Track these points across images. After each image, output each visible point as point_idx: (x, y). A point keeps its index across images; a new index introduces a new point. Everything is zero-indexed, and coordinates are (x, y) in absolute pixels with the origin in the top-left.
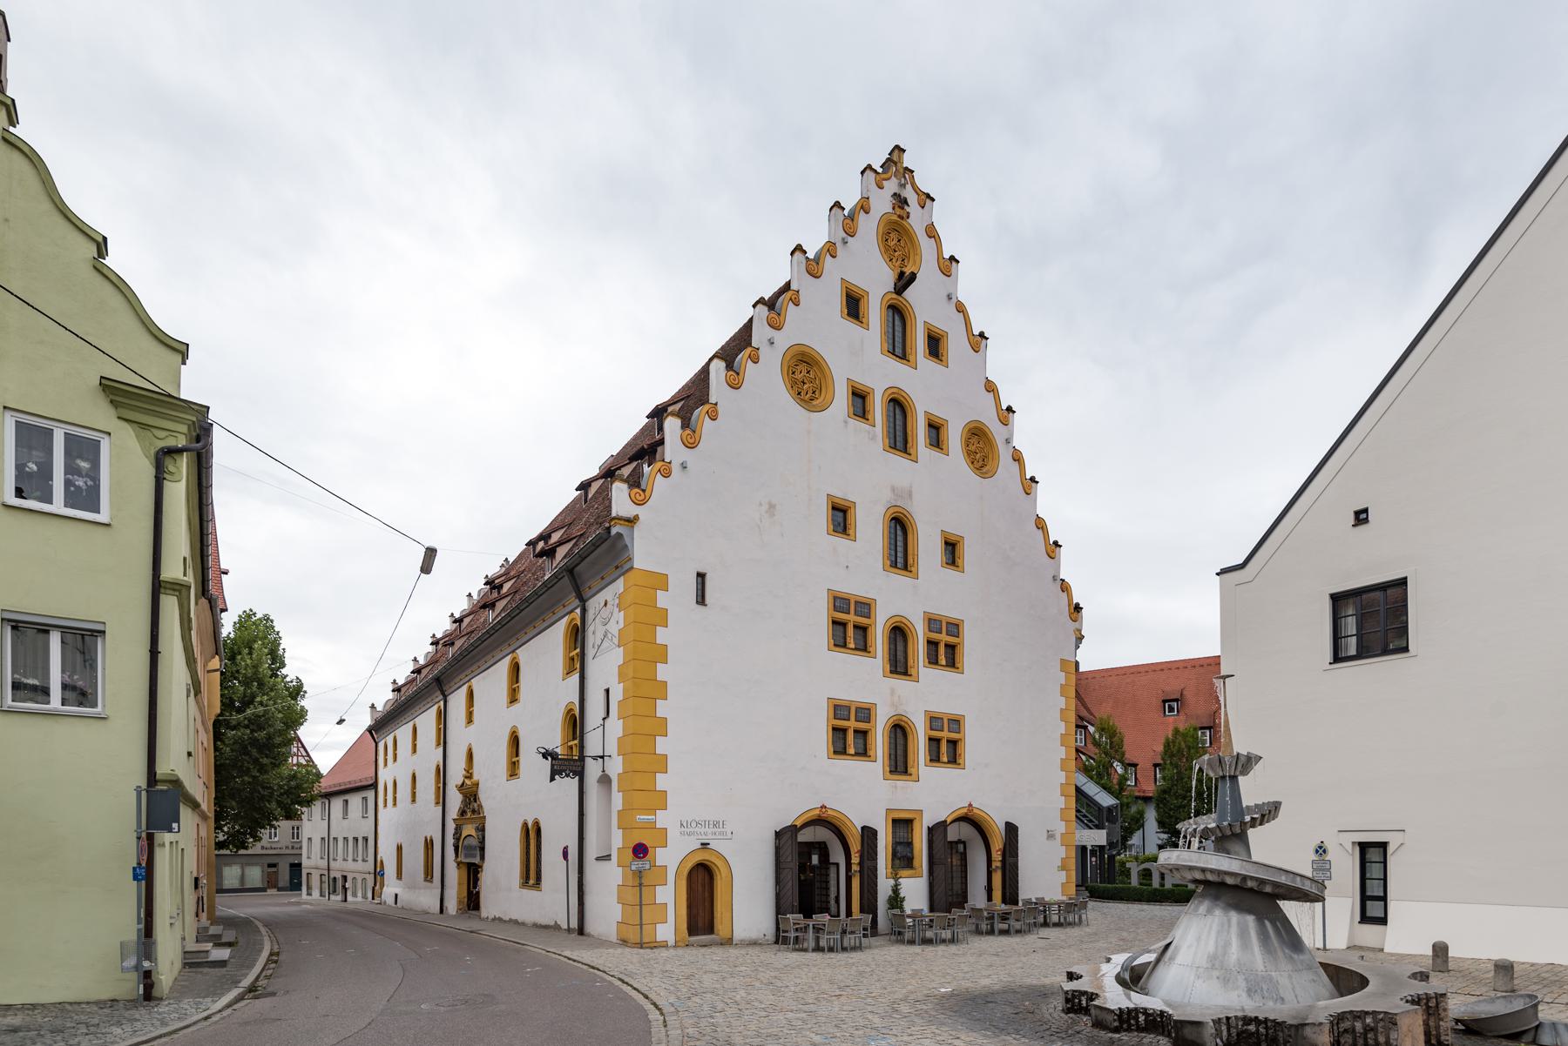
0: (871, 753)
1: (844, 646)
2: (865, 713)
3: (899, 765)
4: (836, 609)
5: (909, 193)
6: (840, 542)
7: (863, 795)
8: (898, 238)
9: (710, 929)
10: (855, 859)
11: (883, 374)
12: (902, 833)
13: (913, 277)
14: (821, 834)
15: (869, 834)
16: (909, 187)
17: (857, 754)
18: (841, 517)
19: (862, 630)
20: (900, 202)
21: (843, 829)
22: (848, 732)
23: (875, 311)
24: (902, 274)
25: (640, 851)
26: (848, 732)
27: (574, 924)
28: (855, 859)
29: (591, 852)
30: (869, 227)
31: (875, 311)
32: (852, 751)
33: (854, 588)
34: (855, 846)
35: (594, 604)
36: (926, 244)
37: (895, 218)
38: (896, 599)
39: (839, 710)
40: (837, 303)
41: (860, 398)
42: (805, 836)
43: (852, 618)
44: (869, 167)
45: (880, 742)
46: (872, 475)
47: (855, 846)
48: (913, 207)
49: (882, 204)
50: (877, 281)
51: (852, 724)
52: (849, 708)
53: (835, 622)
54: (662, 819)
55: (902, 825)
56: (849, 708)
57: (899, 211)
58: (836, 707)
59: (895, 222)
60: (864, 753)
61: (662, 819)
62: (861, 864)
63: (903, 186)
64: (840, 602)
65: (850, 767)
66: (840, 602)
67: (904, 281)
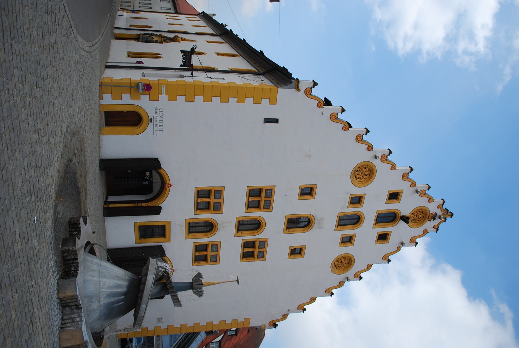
0: (198, 211)
2: (218, 208)
5: (438, 221)
7: (177, 208)
8: (421, 216)
10: (144, 204)
11: (369, 210)
13: (407, 222)
15: (157, 211)
16: (440, 220)
17: (198, 203)
20: (434, 217)
22: (208, 198)
24: (408, 218)
25: (148, 87)
26: (208, 198)
28: (144, 204)
29: (146, 72)
33: (277, 199)
34: (150, 204)
35: (262, 77)
37: (428, 215)
38: (273, 221)
39: (219, 193)
40: (395, 188)
41: (357, 200)
42: (156, 179)
43: (263, 199)
45: (204, 216)
46: (326, 208)
47: (150, 204)
49: (433, 208)
51: (212, 200)
52: (220, 199)
54: (163, 98)
56: (220, 198)
57: (431, 216)
58: (221, 191)
60: (199, 207)
61: (163, 98)
62: (142, 206)
63: (440, 217)
67: (406, 219)
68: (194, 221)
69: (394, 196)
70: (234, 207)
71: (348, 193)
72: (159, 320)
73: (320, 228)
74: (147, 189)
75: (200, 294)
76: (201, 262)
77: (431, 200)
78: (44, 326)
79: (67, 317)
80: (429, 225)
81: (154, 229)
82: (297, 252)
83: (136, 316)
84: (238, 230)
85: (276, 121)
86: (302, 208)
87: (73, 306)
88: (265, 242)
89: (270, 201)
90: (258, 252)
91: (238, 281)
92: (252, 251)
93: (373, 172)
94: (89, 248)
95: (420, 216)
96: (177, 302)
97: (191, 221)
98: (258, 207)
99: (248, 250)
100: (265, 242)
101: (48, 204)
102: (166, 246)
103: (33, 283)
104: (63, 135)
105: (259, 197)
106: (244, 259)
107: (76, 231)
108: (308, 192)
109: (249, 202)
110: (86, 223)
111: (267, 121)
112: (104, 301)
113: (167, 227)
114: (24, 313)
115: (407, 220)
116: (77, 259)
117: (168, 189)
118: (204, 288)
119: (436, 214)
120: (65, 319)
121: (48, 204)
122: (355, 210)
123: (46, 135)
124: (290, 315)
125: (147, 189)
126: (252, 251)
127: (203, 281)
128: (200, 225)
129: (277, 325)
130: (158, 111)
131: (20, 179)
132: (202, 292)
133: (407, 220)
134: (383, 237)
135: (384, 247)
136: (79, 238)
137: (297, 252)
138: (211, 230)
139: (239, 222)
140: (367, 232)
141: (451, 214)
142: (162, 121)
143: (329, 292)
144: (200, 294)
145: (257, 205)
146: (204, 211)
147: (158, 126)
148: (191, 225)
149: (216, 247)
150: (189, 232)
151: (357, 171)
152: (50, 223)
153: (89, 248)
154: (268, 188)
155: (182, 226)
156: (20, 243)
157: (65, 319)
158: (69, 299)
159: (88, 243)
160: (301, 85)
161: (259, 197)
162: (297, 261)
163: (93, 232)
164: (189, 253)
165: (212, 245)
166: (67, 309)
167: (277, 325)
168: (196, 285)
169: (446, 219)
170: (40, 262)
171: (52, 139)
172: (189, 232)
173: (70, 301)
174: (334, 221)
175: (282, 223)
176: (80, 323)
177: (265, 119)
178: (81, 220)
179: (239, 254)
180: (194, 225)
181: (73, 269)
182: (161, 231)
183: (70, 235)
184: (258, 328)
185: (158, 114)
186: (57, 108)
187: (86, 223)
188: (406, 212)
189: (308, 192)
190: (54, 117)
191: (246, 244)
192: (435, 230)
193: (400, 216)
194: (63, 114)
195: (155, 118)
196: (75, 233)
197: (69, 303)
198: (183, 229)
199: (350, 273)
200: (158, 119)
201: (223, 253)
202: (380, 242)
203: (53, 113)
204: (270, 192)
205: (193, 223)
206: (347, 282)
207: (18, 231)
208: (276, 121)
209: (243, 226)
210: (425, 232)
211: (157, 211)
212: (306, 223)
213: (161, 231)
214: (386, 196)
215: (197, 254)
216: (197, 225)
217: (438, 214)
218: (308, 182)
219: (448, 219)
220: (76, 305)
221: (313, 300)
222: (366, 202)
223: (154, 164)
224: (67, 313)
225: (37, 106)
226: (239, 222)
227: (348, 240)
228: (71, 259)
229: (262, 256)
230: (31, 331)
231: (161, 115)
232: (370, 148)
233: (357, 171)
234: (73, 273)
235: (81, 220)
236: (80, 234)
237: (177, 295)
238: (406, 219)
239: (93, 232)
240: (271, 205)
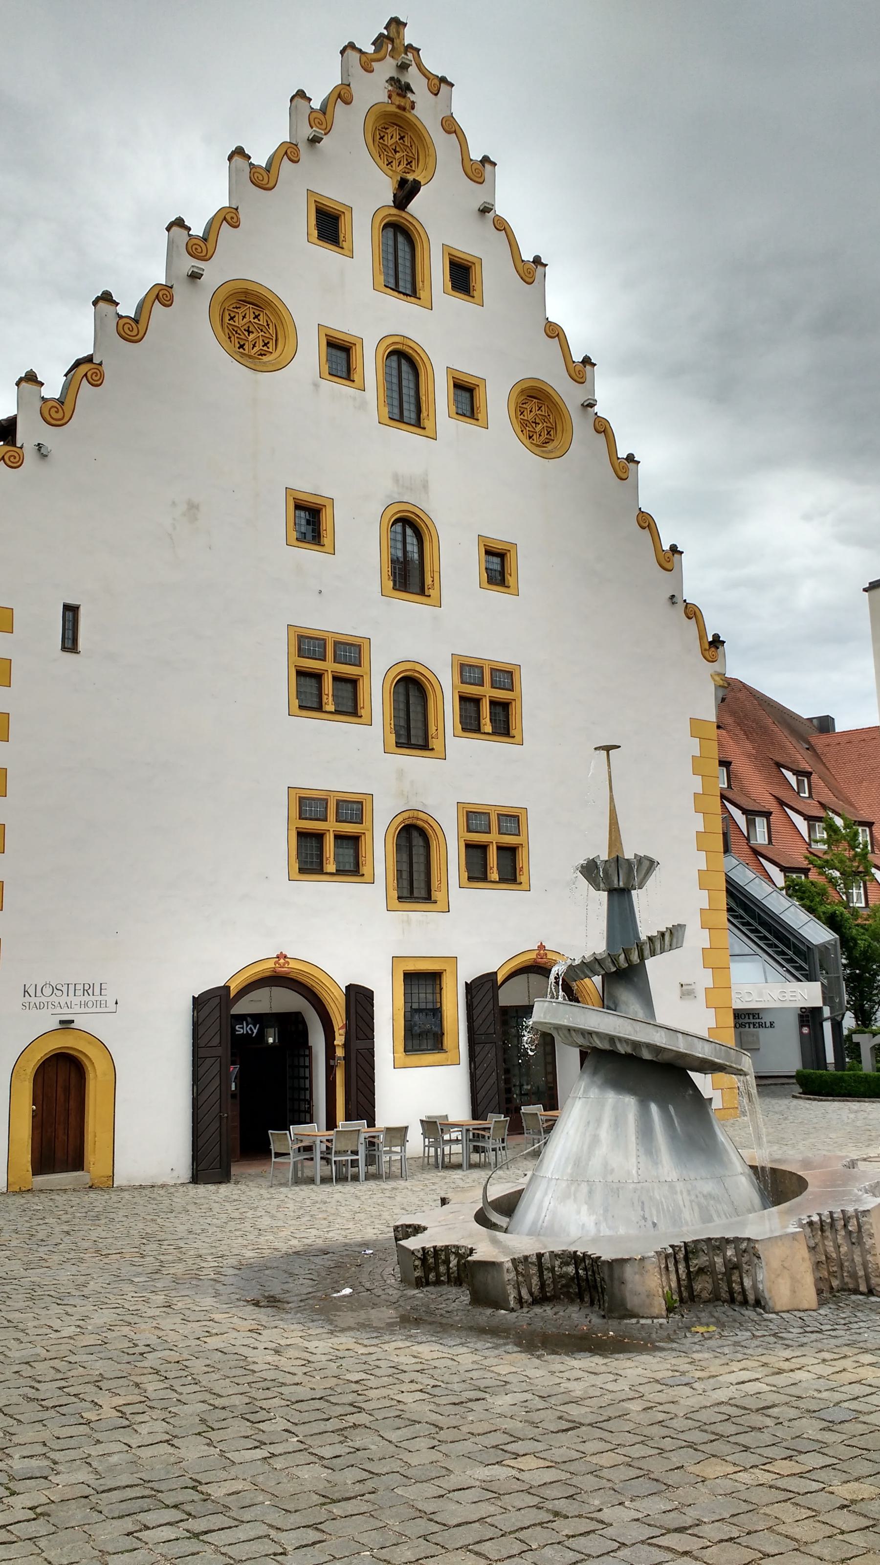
0: (364, 870)
1: (319, 708)
2: (354, 809)
4: (301, 653)
5: (413, 77)
6: (308, 555)
7: (352, 939)
8: (399, 136)
9: (76, 1162)
10: (339, 1040)
11: (375, 318)
12: (423, 997)
14: (285, 1001)
15: (360, 999)
16: (413, 69)
17: (340, 872)
18: (310, 521)
19: (349, 686)
20: (401, 88)
21: (318, 989)
23: (362, 233)
24: (403, 183)
26: (325, 840)
28: (339, 1040)
30: (351, 124)
31: (362, 233)
32: (331, 867)
33: (332, 621)
34: (339, 1019)
36: (442, 144)
37: (393, 109)
38: (400, 636)
40: (302, 222)
41: (340, 354)
43: (329, 667)
44: (351, 46)
47: (339, 1019)
49: (373, 91)
50: (366, 193)
51: (331, 826)
53: (301, 674)
55: (421, 983)
57: (398, 100)
58: (302, 800)
59: (395, 115)
60: (352, 868)
62: (346, 1046)
63: (403, 67)
64: (307, 644)
65: (329, 893)
68: (393, 883)
69: (329, 226)
70: (355, 758)
71: (316, 385)
73: (425, 486)
74: (292, 1027)
75: (648, 865)
76: (519, 864)
77: (342, 95)
78: (765, 1365)
79: (724, 1286)
80: (425, 110)
81: (415, 1006)
82: (498, 566)
83: (707, 1066)
84: (424, 746)
85: (71, 611)
86: (360, 542)
87: (688, 1267)
88: (462, 666)
89: (336, 644)
90: (492, 687)
91: (608, 749)
92: (491, 708)
93: (246, 292)
94: (495, 1217)
95: (396, 138)
96: (670, 938)
97: (395, 894)
98: (353, 683)
100: (462, 666)
101: (369, 1359)
102: (468, 972)
103: (635, 1406)
104: (128, 1318)
105: (325, 678)
106: (513, 732)
107: (447, 1262)
108: (310, 521)
109: (337, 712)
110: (418, 1230)
111: (70, 642)
112: (668, 1167)
113: (412, 967)
114: (741, 1439)
115: (408, 187)
116: (540, 1256)
117: (293, 964)
118: (629, 855)
119: (391, 80)
120: (731, 1292)
121: (369, 1359)
122: (370, 365)
123: (137, 1385)
124: (690, 593)
125: (292, 1027)
126: (491, 708)
127: (605, 857)
128: (405, 867)
129: (716, 637)
130: (33, 1000)
131: (305, 1473)
132: (640, 860)
133: (408, 187)
134: (462, 276)
135: (493, 275)
136: (472, 1251)
137: (498, 566)
138: (423, 833)
139: (398, 745)
140: (445, 333)
141: (393, 26)
142: (71, 988)
143: (626, 470)
144: (648, 865)
145: (349, 687)
146: (362, 852)
147: (86, 998)
148: (406, 893)
149: (474, 818)
150: (428, 898)
151: (242, 346)
152: (428, 1350)
153: (495, 1217)
154: (294, 650)
155: (409, 922)
156: (521, 1463)
157: (731, 1292)
158: (669, 1280)
159: (481, 1218)
161: (325, 678)
162: (524, 567)
163: (444, 1201)
164: (493, 899)
166: (697, 1287)
167: (716, 637)
168: (617, 878)
169: (410, 46)
170: (566, 1385)
171: (152, 1360)
172: (428, 898)
173: (673, 1277)
174: (404, 438)
175: (407, 607)
176: (744, 1245)
177: (64, 648)
178: (413, 1243)
179: (498, 748)
180: (406, 884)
181: (571, 1270)
182: (422, 982)
183: (458, 1282)
184: (720, 696)
186: (39, 1350)
187: (418, 1230)
188: (383, 190)
190: (72, 1358)
191: (470, 724)
193: (394, 211)
194: (57, 1324)
195: (58, 1010)
196: (454, 1261)
197: (679, 1280)
200: (63, 999)
201: (493, 796)
202: (477, 287)
203: (57, 1363)
204: (307, 644)
205: (399, 888)
206: (596, 409)
207: (483, 1473)
208: (71, 611)
210: (450, 126)
211: (360, 999)
212: (409, 531)
213: (422, 982)
214: (325, 253)
215: (494, 875)
216: (405, 875)
217: (393, 73)
218: (279, 519)
220: (687, 1259)
222: (346, 326)
223: (212, 1011)
224: (710, 1287)
225: (39, 1426)
226: (398, 745)
227: (466, 394)
228: (541, 1276)
229: (505, 677)
230: (793, 1413)
231: (48, 991)
232: (162, 295)
233: (242, 346)
234: (585, 1269)
235: (413, 1243)
236: (457, 1247)
237: (650, 939)
239: (444, 1201)
240: (350, 640)
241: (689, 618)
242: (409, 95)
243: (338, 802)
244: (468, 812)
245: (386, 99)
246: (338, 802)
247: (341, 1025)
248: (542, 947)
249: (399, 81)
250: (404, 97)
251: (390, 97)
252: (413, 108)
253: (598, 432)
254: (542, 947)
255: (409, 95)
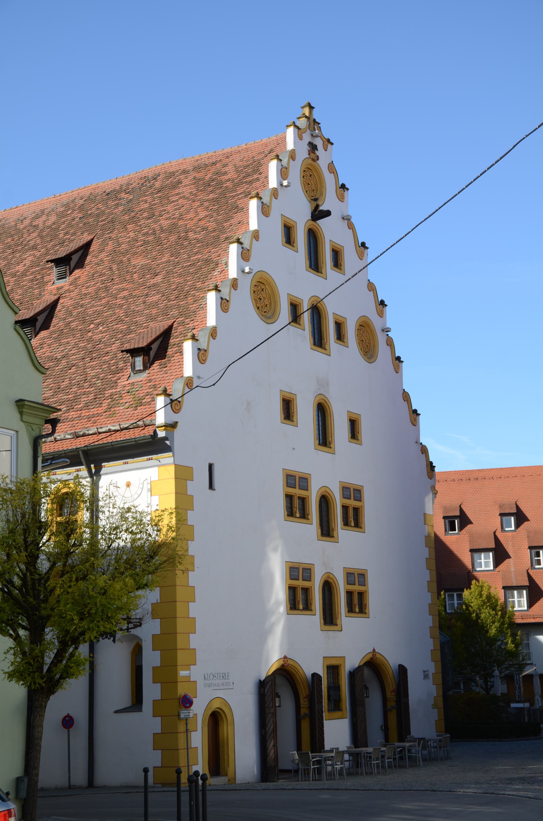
3: (329, 618)
5: (318, 142)
10: (304, 703)
20: (313, 147)
27: (80, 777)
32: (301, 607)
33: (299, 467)
34: (303, 692)
48: (320, 152)
52: (298, 568)
57: (312, 154)
60: (308, 607)
64: (291, 479)
66: (291, 479)
67: (319, 214)
72: (426, 677)
85: (211, 466)
89: (300, 478)
99: (352, 519)
108: (288, 409)
117: (290, 662)
124: (424, 440)
130: (208, 682)
147: (224, 681)
160: (170, 422)
165: (348, 584)
174: (318, 355)
175: (323, 455)
185: (210, 682)
189: (288, 409)
192: (329, 145)
198: (332, 634)
199: (376, 323)
201: (356, 564)
202: (342, 264)
208: (211, 466)
209: (326, 531)
210: (332, 168)
213: (333, 670)
219: (316, 115)
221: (406, 397)
227: (339, 326)
231: (211, 676)
238: (319, 214)
241: (423, 453)
242: (316, 152)
243: (303, 569)
244: (348, 573)
245: (307, 156)
246: (303, 569)
247: (305, 696)
248: (374, 650)
249: (312, 143)
250: (315, 153)
251: (309, 154)
252: (318, 159)
253: (388, 345)
254: (374, 650)
255: (316, 152)
